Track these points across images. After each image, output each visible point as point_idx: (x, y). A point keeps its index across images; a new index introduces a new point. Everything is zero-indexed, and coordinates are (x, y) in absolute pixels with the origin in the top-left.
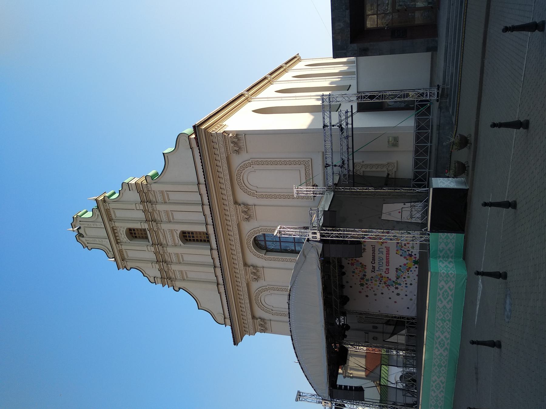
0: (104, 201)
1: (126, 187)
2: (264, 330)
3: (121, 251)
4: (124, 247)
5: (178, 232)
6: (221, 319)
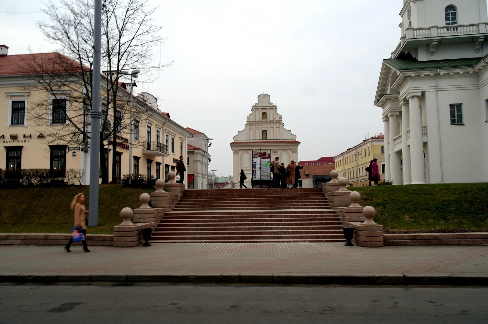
0: (276, 108)
1: (280, 117)
2: (234, 153)
3: (259, 109)
4: (260, 111)
5: (266, 130)
6: (236, 138)
